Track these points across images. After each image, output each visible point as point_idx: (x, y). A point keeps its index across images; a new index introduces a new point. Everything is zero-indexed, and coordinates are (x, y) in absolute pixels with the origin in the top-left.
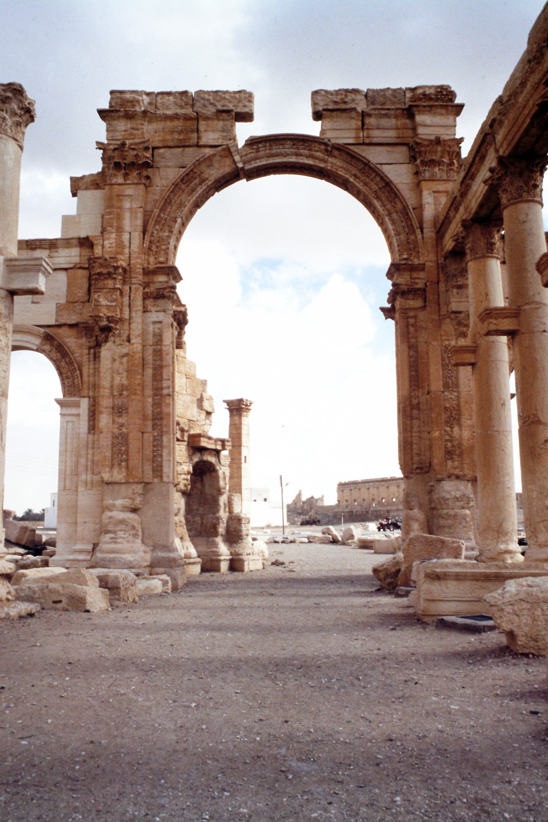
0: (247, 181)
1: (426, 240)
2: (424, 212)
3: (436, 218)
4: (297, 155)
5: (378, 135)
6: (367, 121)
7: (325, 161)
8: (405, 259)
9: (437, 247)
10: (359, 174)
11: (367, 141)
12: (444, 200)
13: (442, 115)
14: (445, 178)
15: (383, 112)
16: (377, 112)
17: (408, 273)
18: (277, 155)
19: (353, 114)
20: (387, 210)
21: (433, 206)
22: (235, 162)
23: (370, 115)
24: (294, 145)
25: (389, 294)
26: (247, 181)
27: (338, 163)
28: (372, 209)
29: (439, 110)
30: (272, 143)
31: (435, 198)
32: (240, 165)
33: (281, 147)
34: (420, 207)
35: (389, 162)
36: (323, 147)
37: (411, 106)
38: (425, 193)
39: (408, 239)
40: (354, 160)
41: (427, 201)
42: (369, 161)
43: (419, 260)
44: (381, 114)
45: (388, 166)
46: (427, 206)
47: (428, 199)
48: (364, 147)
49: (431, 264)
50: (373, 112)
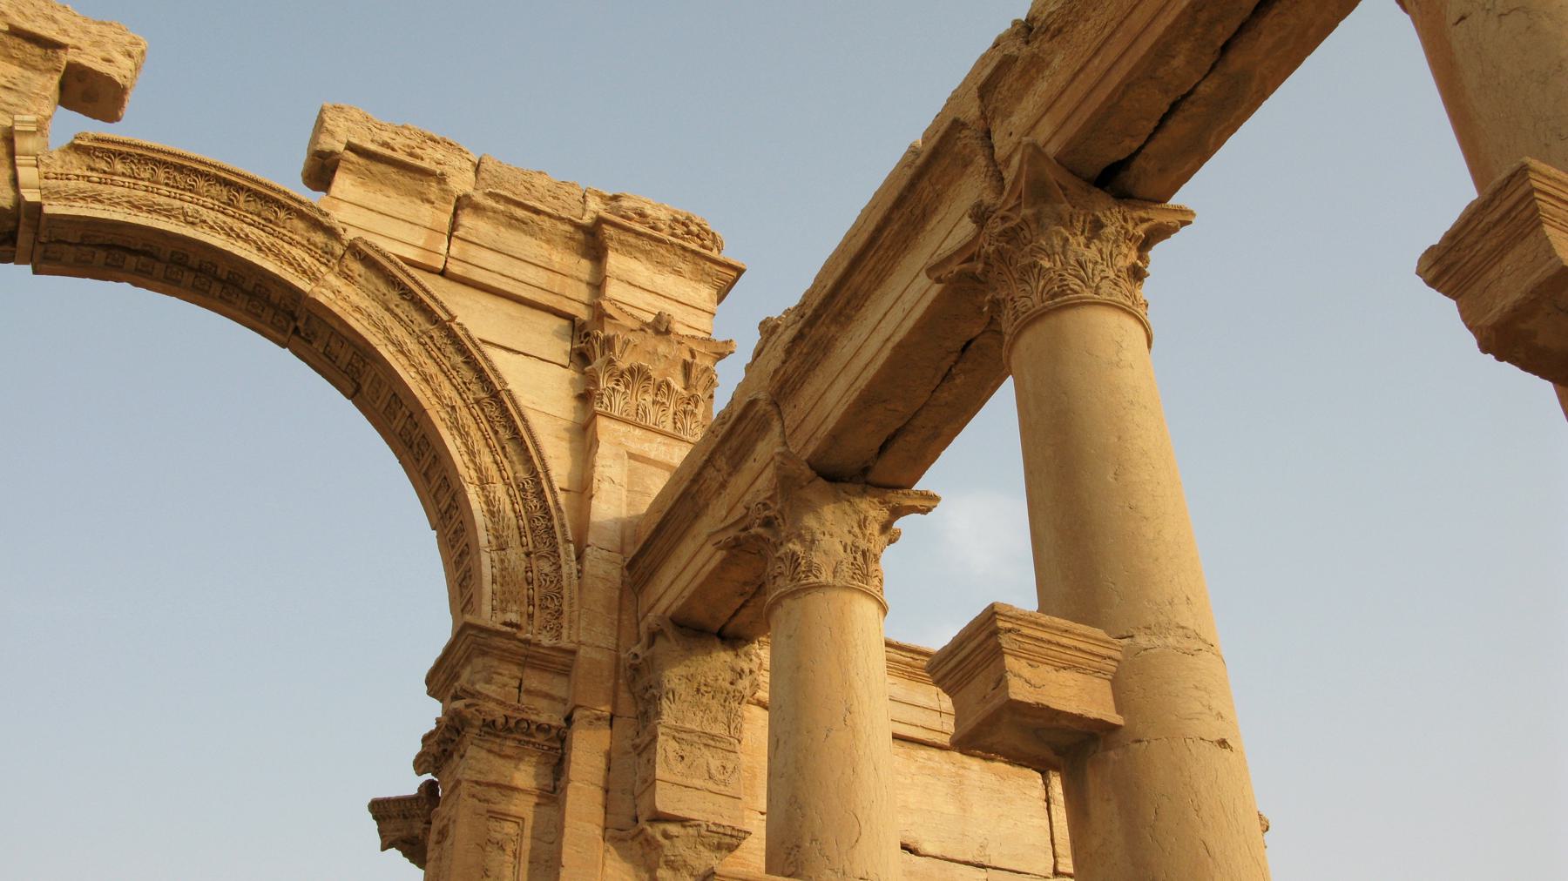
0: (36, 272)
1: (588, 580)
2: (594, 502)
3: (627, 527)
4: (230, 233)
5: (489, 266)
6: (467, 220)
7: (314, 278)
8: (511, 624)
9: (620, 610)
10: (411, 345)
11: (455, 268)
12: (656, 483)
13: (679, 273)
14: (669, 428)
15: (520, 213)
16: (501, 207)
17: (515, 670)
18: (168, 213)
19: (433, 190)
20: (478, 470)
21: (624, 493)
22: (15, 182)
23: (477, 209)
24: (230, 203)
25: (426, 739)
26: (36, 272)
27: (355, 299)
28: (427, 460)
29: (671, 258)
30: (161, 175)
31: (632, 472)
32: (31, 196)
33: (187, 195)
34: (583, 489)
35: (508, 346)
36: (319, 238)
37: (600, 221)
38: (605, 451)
39: (529, 569)
40: (405, 305)
41: (608, 472)
42: (453, 318)
43: (558, 637)
44: (512, 217)
45: (503, 353)
46: (605, 486)
47: (609, 467)
48: (441, 281)
49: (598, 656)
50: (490, 203)
